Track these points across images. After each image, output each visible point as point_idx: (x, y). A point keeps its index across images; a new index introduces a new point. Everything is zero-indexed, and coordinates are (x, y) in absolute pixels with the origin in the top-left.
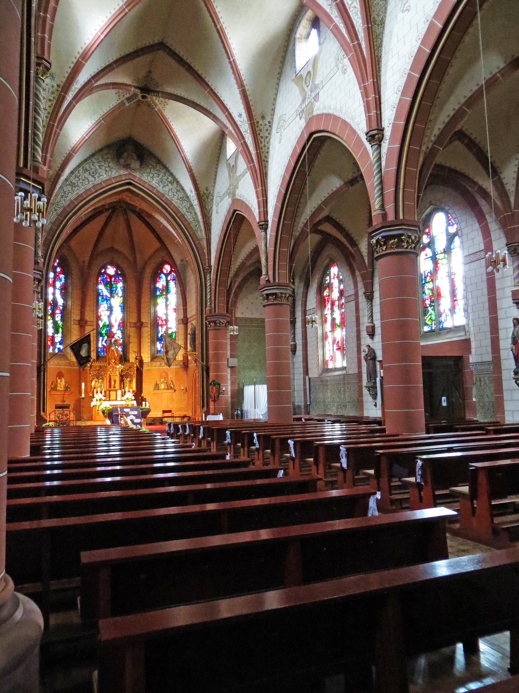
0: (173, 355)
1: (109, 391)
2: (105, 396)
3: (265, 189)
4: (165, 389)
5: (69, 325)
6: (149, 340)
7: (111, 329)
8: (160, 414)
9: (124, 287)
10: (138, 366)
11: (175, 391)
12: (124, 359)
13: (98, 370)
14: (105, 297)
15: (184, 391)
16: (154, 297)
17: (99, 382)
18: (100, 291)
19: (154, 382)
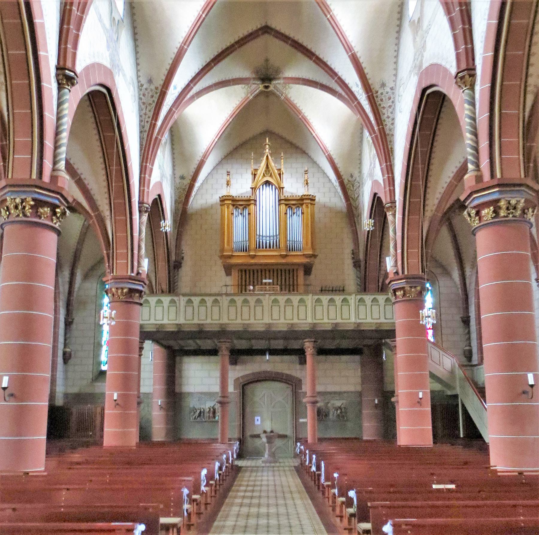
3: (391, 166)
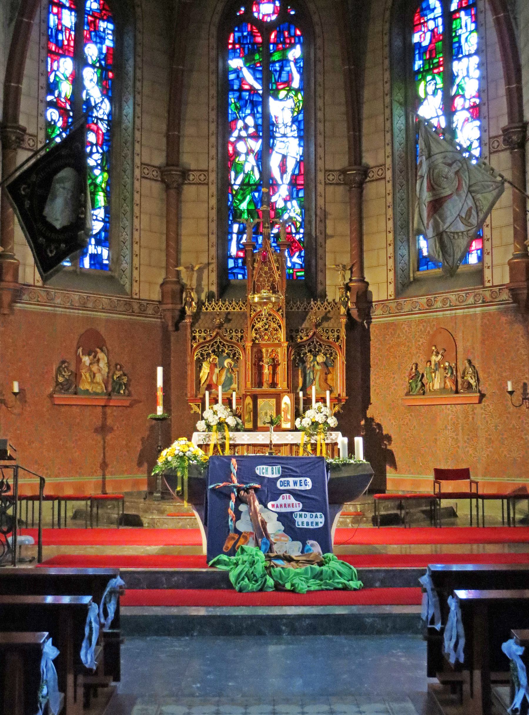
0: (466, 220)
1: (255, 398)
2: (235, 415)
4: (444, 390)
5: (129, 181)
6: (390, 224)
7: (266, 199)
8: (427, 486)
9: (305, 57)
10: (354, 313)
11: (482, 396)
12: (305, 289)
13: (220, 326)
14: (246, 95)
15: (518, 397)
16: (408, 79)
17: (223, 368)
18: (232, 77)
19: (410, 365)
